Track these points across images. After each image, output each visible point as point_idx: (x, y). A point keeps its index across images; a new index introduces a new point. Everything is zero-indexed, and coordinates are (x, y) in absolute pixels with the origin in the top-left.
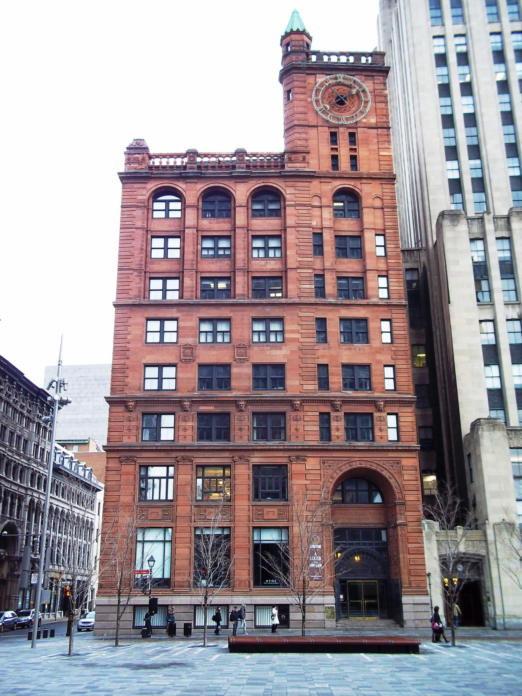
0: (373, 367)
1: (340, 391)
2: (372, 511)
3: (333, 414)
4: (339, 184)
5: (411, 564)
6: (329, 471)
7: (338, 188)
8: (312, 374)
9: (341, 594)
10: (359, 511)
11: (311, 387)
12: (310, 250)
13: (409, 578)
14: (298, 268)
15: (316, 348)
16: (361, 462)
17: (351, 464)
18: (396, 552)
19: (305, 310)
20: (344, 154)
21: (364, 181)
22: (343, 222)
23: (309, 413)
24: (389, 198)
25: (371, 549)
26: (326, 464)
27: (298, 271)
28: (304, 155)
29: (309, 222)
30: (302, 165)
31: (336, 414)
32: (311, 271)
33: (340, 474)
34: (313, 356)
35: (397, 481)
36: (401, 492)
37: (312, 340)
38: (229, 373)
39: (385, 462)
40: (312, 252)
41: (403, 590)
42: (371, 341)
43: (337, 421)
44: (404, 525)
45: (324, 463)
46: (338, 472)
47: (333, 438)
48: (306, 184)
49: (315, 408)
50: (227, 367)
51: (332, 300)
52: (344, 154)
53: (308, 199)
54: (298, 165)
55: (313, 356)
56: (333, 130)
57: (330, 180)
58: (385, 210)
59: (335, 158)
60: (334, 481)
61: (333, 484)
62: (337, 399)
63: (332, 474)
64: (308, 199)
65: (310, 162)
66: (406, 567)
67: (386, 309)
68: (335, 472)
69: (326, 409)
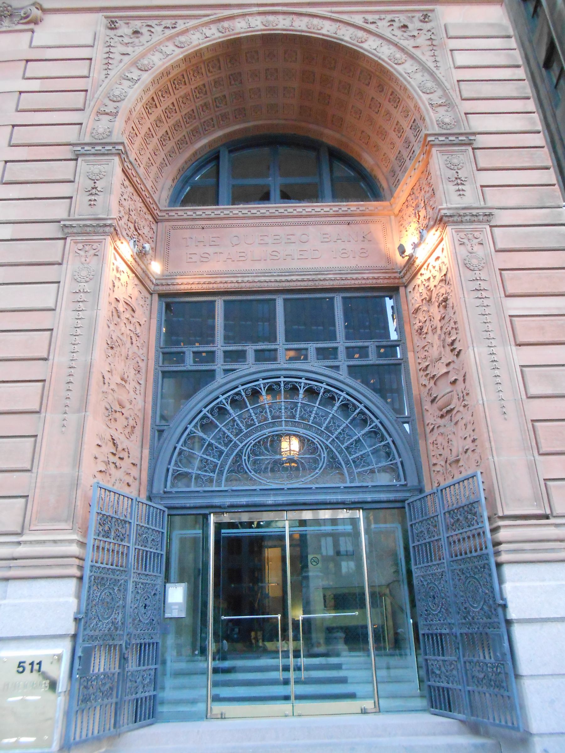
2: (328, 229)
5: (533, 391)
6: (129, 50)
9: (181, 580)
10: (278, 230)
13: (533, 468)
16: (271, 18)
17: (226, 24)
18: (449, 357)
25: (328, 372)
26: (125, 30)
33: (178, 54)
35: (424, 68)
36: (448, 104)
39: (370, 18)
41: (502, 535)
44: (474, 219)
45: (112, 26)
46: (170, 48)
60: (147, 77)
61: (138, 89)
63: (143, 56)
66: (510, 408)
68: (154, 49)
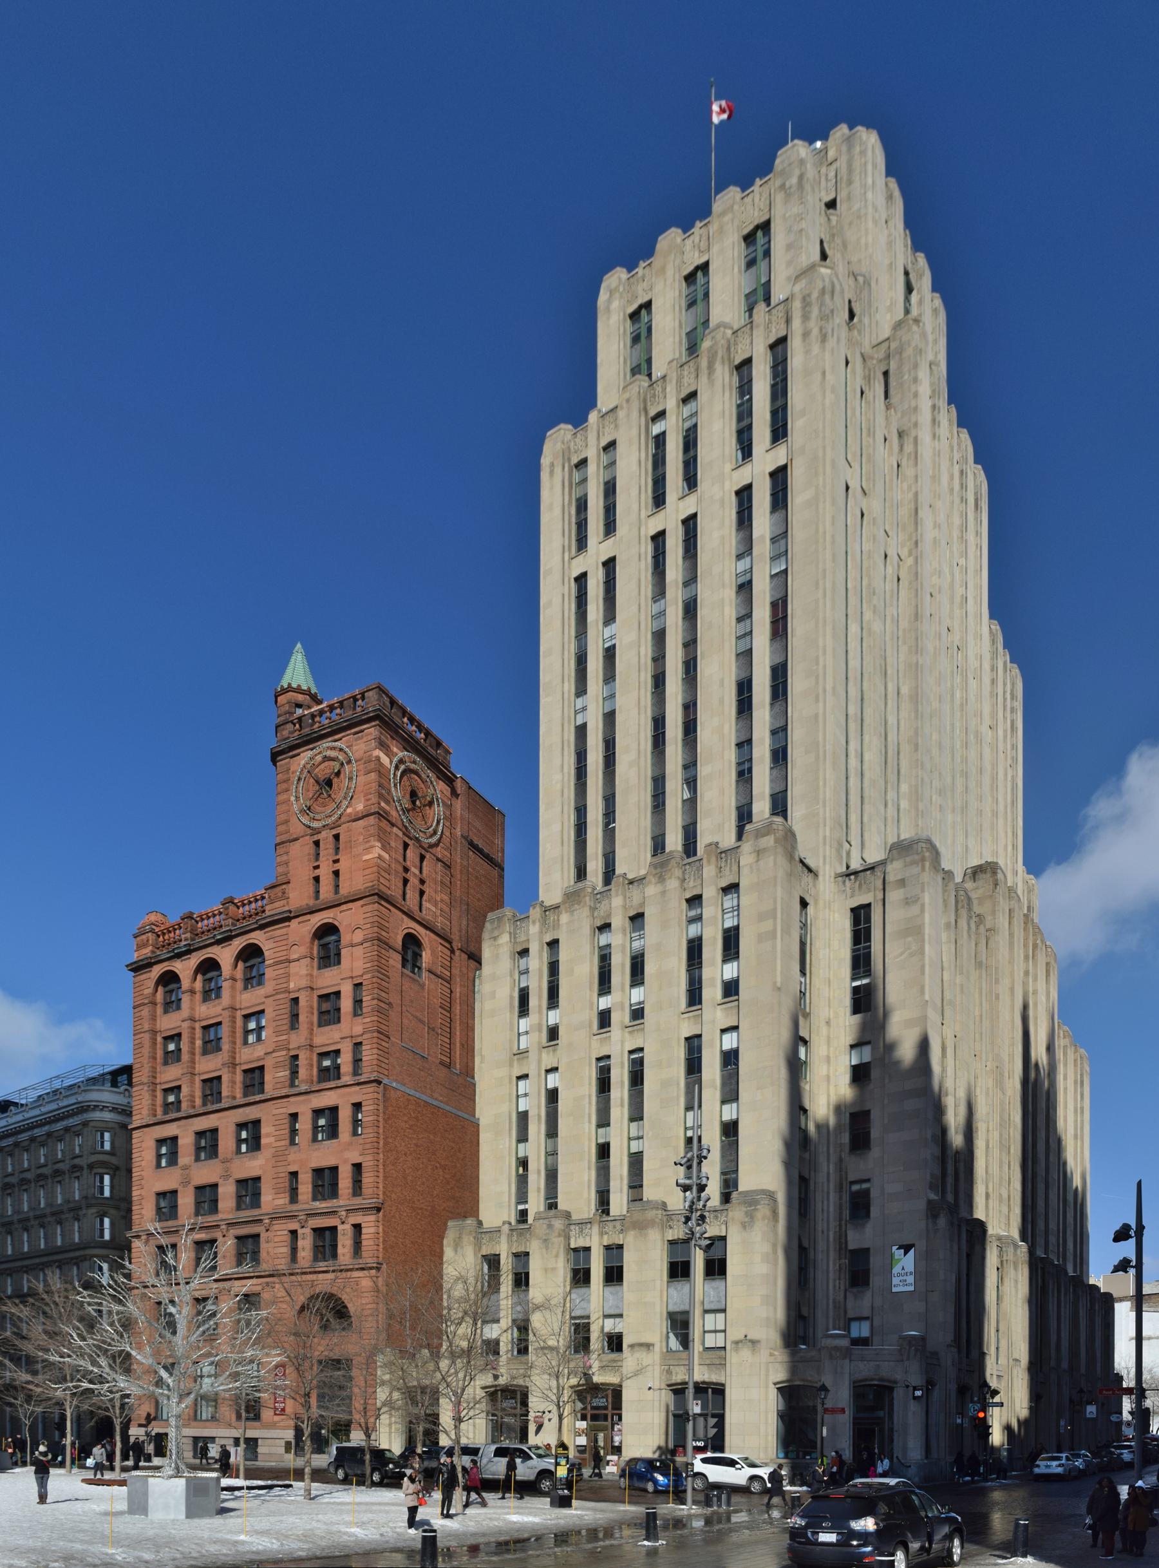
0: (340, 1169)
1: (307, 1203)
3: (300, 1231)
4: (317, 920)
7: (316, 927)
8: (282, 1185)
11: (281, 1202)
12: (286, 1021)
14: (273, 1052)
15: (287, 1152)
19: (278, 1106)
20: (325, 872)
21: (344, 907)
22: (326, 974)
23: (279, 1233)
24: (369, 926)
27: (274, 1055)
28: (284, 886)
29: (285, 985)
30: (282, 903)
31: (304, 1230)
32: (284, 1053)
34: (284, 1163)
37: (283, 1143)
38: (216, 1193)
40: (285, 1027)
42: (340, 1135)
43: (303, 1239)
47: (299, 1259)
48: (284, 931)
49: (284, 1227)
50: (215, 1186)
51: (304, 1088)
52: (325, 872)
53: (285, 953)
54: (277, 905)
55: (284, 1163)
56: (316, 838)
57: (308, 917)
58: (365, 945)
59: (317, 879)
62: (301, 1213)
64: (285, 953)
65: (291, 895)
67: (357, 1088)
69: (294, 1226)
